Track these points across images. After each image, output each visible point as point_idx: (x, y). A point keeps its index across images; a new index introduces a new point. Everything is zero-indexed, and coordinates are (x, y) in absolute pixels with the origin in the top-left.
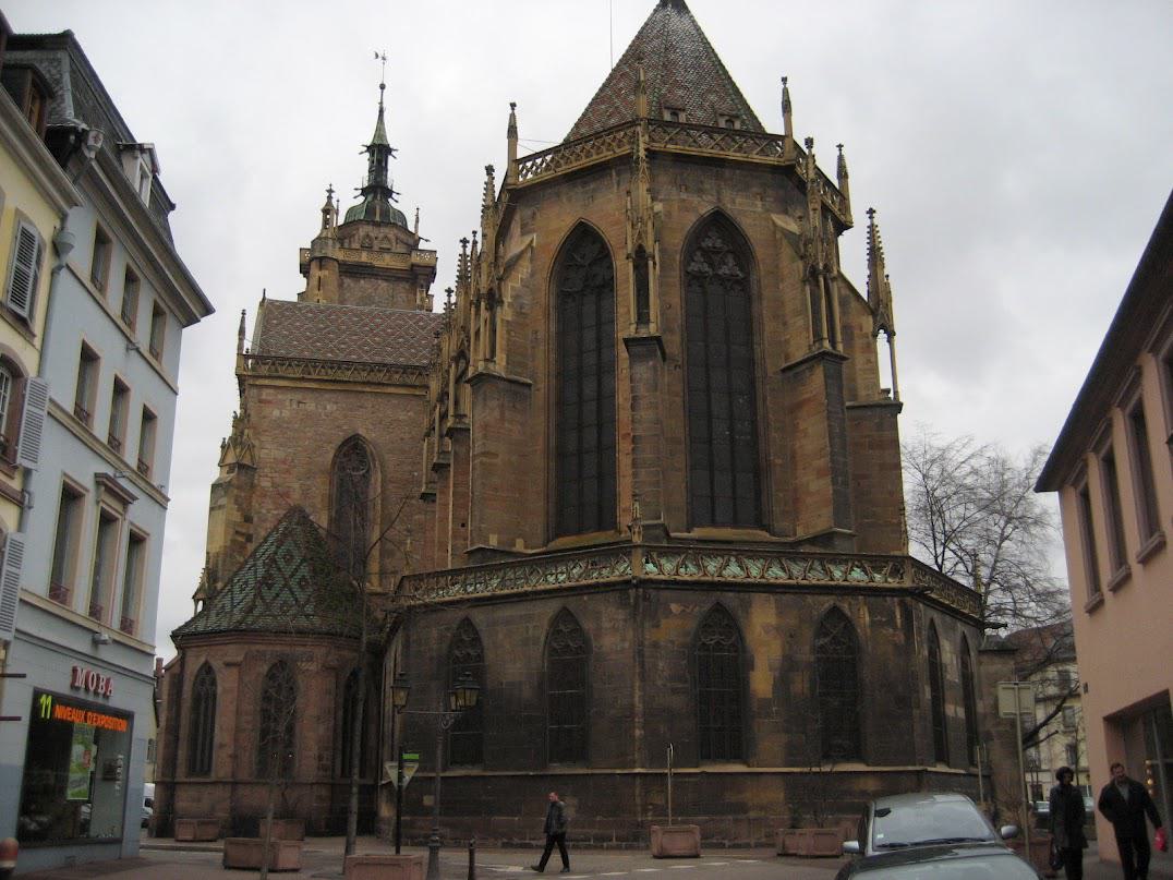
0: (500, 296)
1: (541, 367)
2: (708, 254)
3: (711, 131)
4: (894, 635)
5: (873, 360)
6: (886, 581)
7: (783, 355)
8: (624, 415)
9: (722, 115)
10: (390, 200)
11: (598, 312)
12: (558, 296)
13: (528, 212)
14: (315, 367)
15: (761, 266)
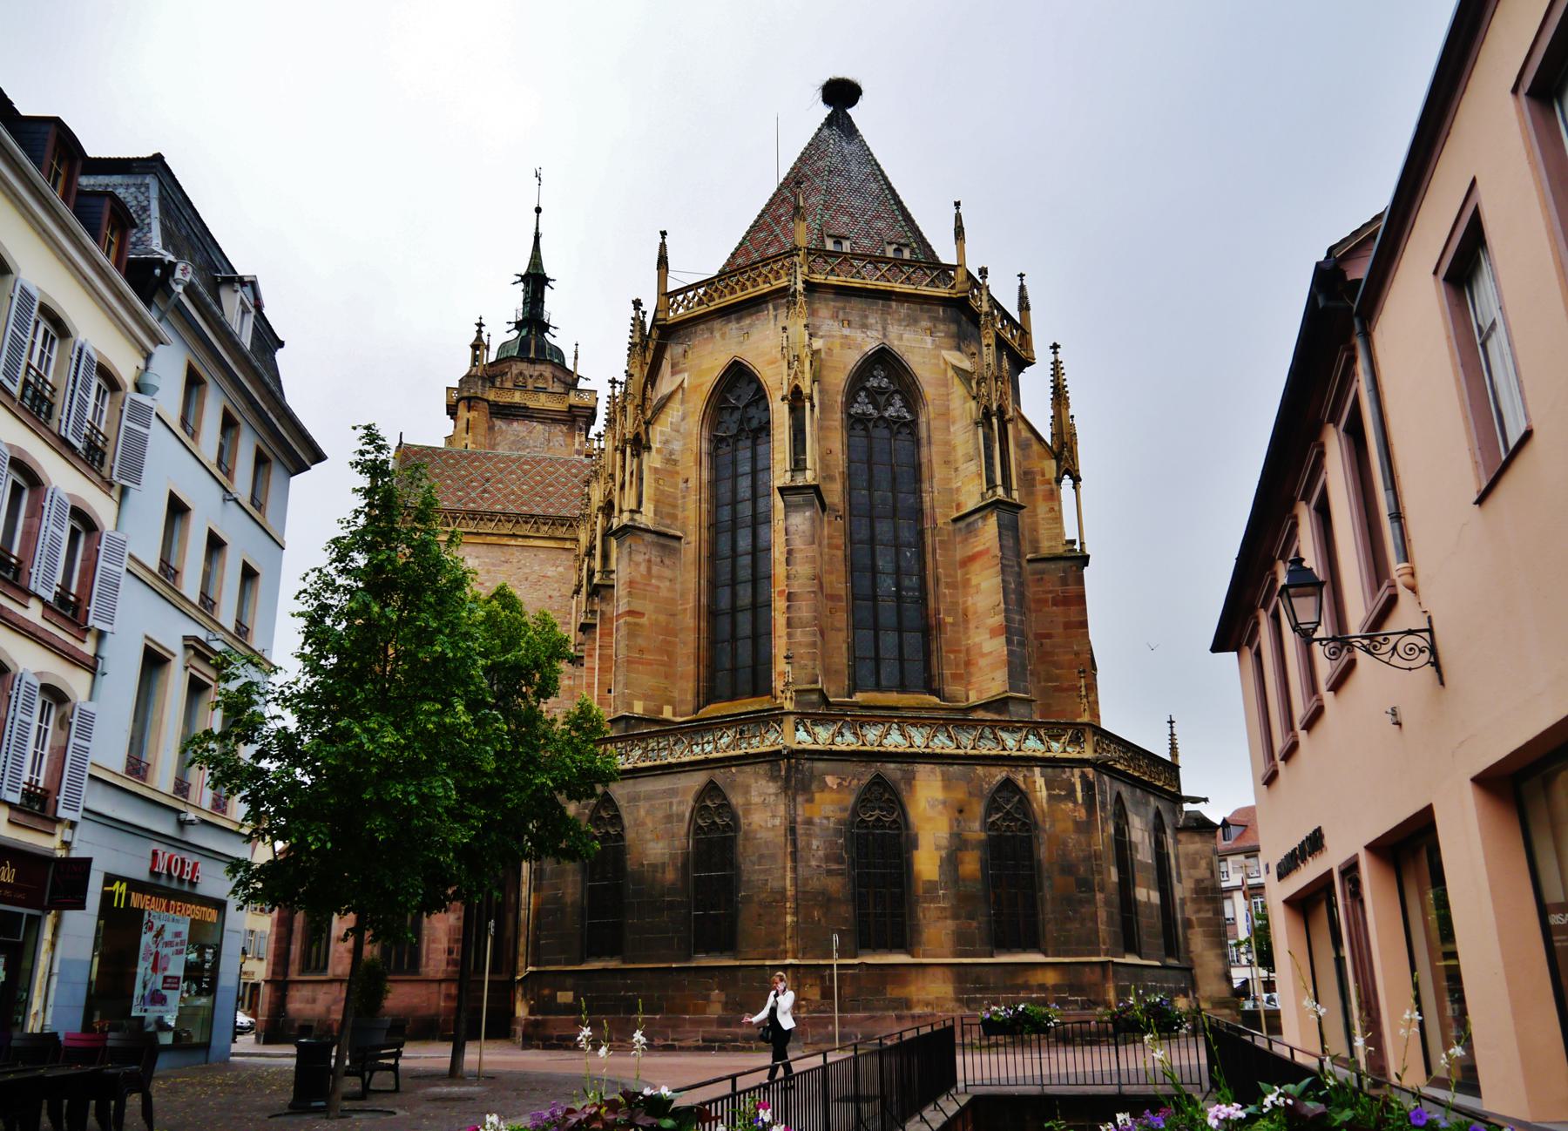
0: (648, 440)
1: (691, 518)
2: (873, 395)
3: (875, 261)
4: (1075, 811)
5: (1056, 508)
6: (1065, 751)
7: (954, 505)
8: (779, 570)
9: (890, 243)
10: (546, 334)
11: (754, 459)
12: (710, 441)
13: (679, 350)
14: (455, 519)
15: (930, 408)
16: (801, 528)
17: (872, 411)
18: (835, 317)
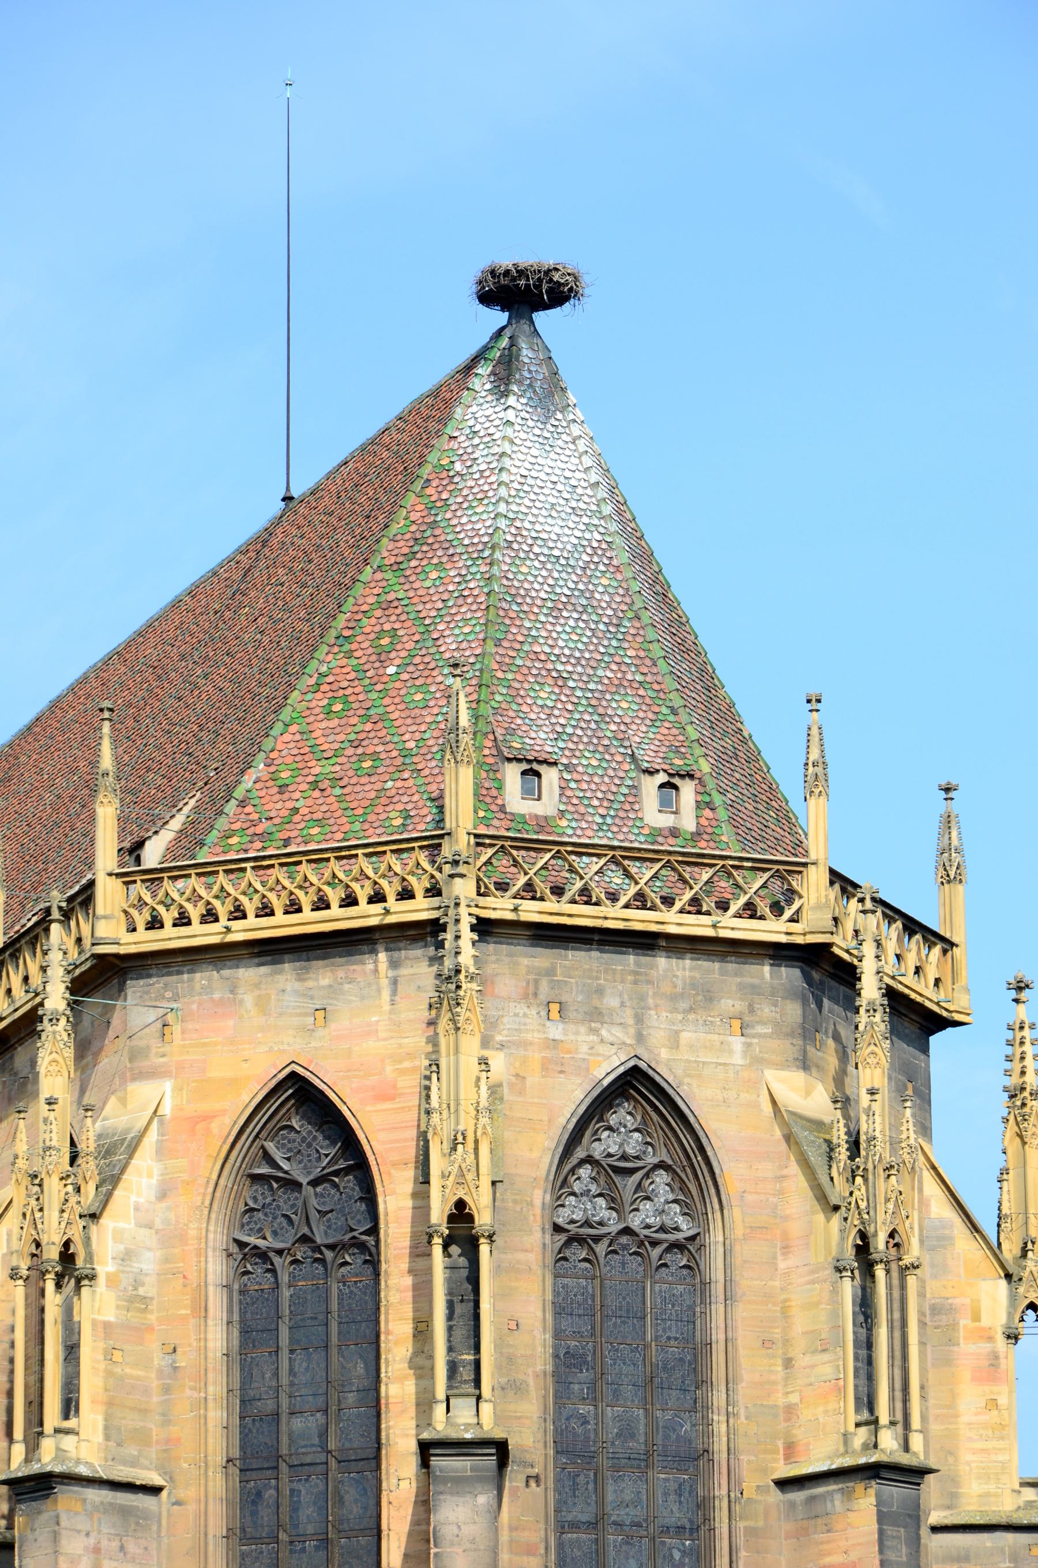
0: (90, 1257)
7: (780, 1444)
9: (651, 772)
16: (468, 1530)
17: (605, 1214)
18: (529, 995)
